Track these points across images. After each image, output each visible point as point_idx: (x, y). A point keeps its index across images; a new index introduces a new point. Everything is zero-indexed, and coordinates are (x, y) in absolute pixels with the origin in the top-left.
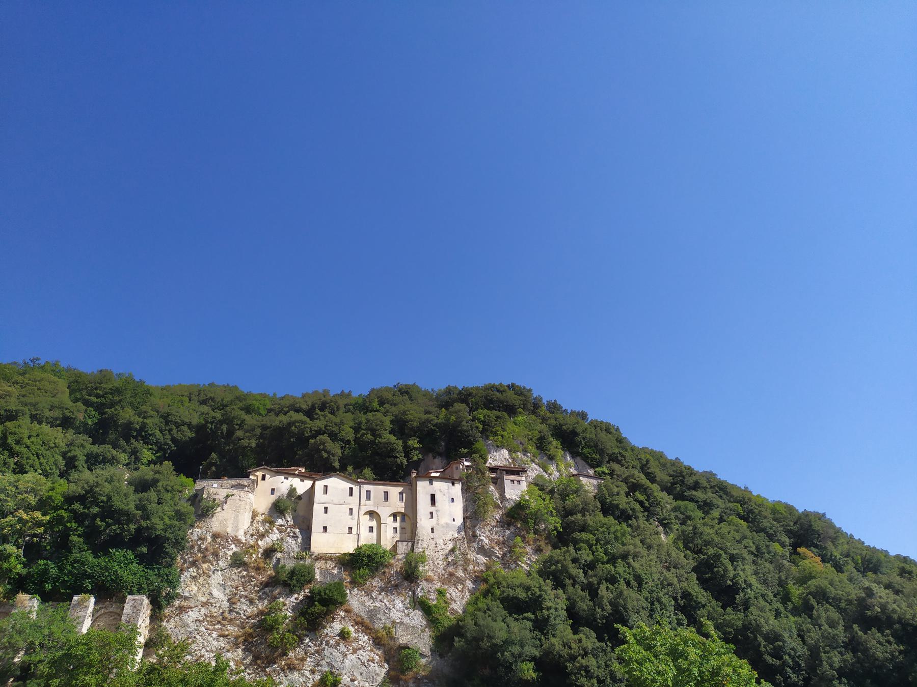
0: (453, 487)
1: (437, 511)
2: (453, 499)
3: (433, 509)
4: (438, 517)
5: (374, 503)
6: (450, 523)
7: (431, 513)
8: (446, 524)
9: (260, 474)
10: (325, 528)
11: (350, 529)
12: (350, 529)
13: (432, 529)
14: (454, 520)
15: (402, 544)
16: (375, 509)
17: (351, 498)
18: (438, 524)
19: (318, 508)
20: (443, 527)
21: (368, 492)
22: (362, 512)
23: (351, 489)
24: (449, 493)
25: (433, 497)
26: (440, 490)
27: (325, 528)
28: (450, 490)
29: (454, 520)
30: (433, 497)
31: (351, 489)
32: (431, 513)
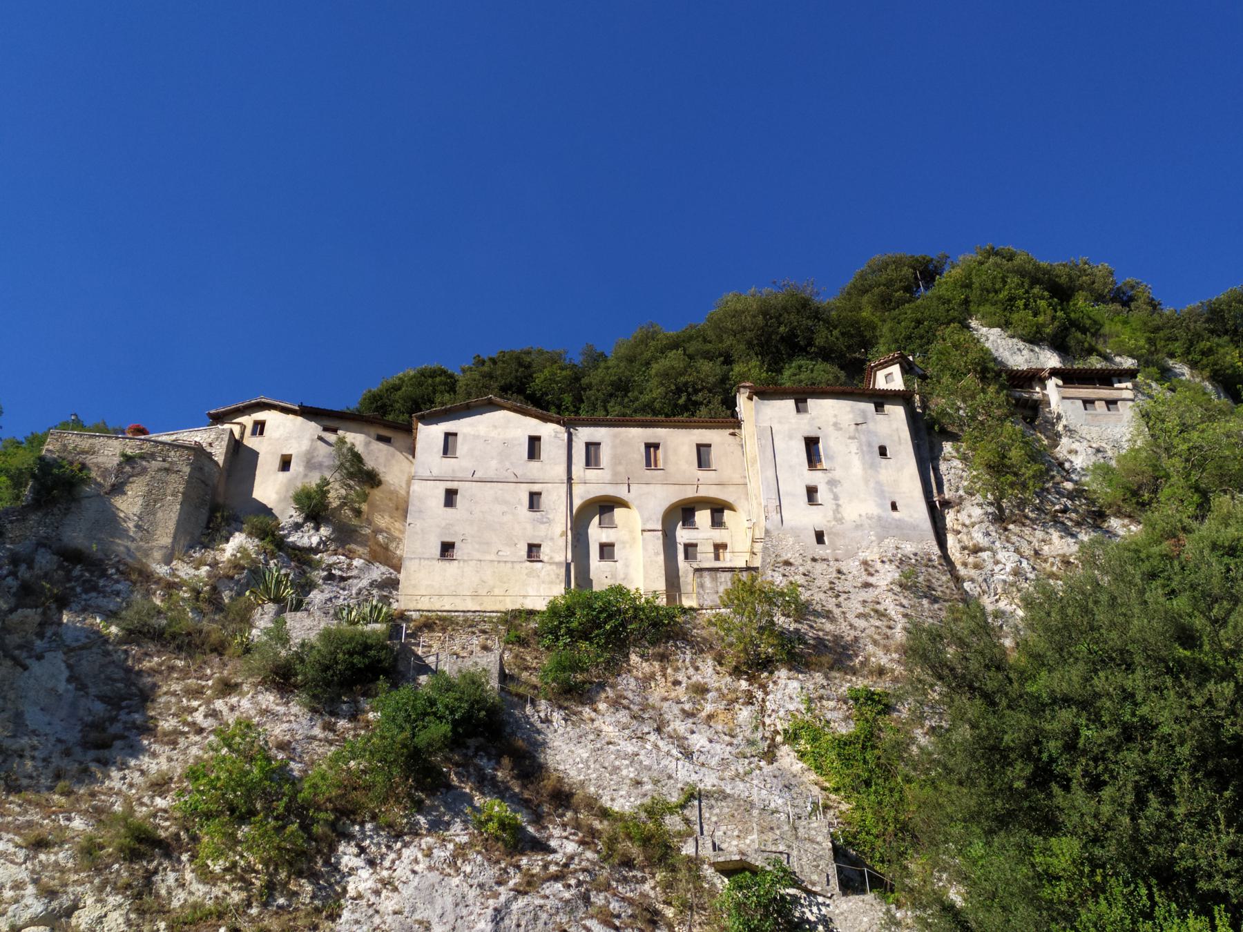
0: (880, 417)
1: (832, 483)
2: (883, 451)
3: (816, 478)
4: (836, 498)
5: (615, 474)
6: (883, 514)
7: (811, 492)
8: (870, 518)
9: (248, 420)
10: (447, 549)
11: (533, 550)
12: (533, 550)
13: (820, 537)
14: (894, 507)
15: (715, 579)
16: (620, 492)
17: (534, 464)
18: (840, 520)
19: (428, 496)
20: (858, 527)
21: (592, 448)
22: (577, 503)
23: (534, 441)
24: (869, 432)
25: (811, 444)
26: (835, 424)
27: (447, 549)
28: (871, 425)
29: (894, 507)
30: (811, 444)
31: (534, 441)
32: (811, 492)
